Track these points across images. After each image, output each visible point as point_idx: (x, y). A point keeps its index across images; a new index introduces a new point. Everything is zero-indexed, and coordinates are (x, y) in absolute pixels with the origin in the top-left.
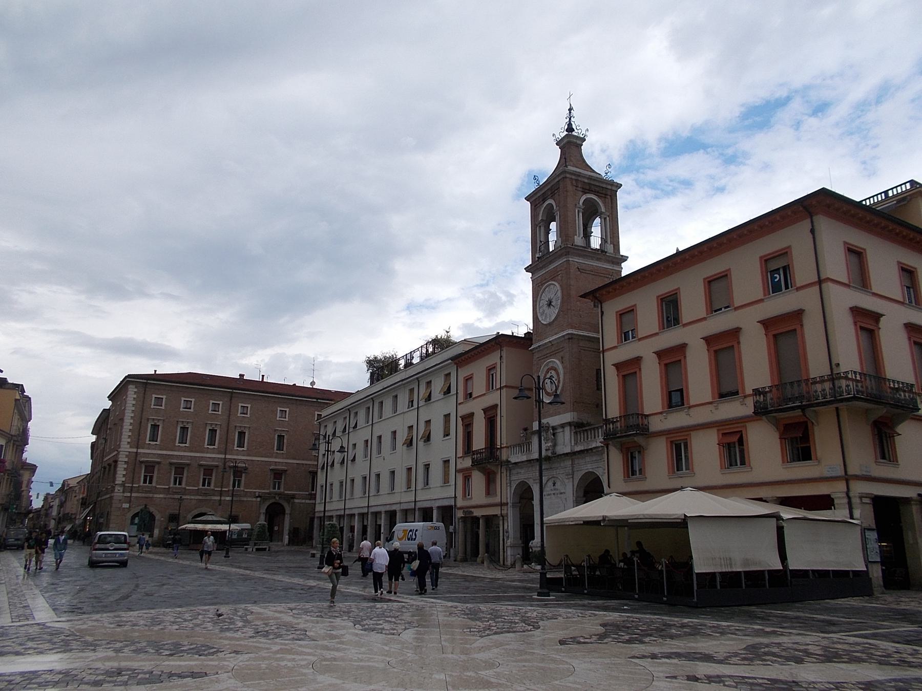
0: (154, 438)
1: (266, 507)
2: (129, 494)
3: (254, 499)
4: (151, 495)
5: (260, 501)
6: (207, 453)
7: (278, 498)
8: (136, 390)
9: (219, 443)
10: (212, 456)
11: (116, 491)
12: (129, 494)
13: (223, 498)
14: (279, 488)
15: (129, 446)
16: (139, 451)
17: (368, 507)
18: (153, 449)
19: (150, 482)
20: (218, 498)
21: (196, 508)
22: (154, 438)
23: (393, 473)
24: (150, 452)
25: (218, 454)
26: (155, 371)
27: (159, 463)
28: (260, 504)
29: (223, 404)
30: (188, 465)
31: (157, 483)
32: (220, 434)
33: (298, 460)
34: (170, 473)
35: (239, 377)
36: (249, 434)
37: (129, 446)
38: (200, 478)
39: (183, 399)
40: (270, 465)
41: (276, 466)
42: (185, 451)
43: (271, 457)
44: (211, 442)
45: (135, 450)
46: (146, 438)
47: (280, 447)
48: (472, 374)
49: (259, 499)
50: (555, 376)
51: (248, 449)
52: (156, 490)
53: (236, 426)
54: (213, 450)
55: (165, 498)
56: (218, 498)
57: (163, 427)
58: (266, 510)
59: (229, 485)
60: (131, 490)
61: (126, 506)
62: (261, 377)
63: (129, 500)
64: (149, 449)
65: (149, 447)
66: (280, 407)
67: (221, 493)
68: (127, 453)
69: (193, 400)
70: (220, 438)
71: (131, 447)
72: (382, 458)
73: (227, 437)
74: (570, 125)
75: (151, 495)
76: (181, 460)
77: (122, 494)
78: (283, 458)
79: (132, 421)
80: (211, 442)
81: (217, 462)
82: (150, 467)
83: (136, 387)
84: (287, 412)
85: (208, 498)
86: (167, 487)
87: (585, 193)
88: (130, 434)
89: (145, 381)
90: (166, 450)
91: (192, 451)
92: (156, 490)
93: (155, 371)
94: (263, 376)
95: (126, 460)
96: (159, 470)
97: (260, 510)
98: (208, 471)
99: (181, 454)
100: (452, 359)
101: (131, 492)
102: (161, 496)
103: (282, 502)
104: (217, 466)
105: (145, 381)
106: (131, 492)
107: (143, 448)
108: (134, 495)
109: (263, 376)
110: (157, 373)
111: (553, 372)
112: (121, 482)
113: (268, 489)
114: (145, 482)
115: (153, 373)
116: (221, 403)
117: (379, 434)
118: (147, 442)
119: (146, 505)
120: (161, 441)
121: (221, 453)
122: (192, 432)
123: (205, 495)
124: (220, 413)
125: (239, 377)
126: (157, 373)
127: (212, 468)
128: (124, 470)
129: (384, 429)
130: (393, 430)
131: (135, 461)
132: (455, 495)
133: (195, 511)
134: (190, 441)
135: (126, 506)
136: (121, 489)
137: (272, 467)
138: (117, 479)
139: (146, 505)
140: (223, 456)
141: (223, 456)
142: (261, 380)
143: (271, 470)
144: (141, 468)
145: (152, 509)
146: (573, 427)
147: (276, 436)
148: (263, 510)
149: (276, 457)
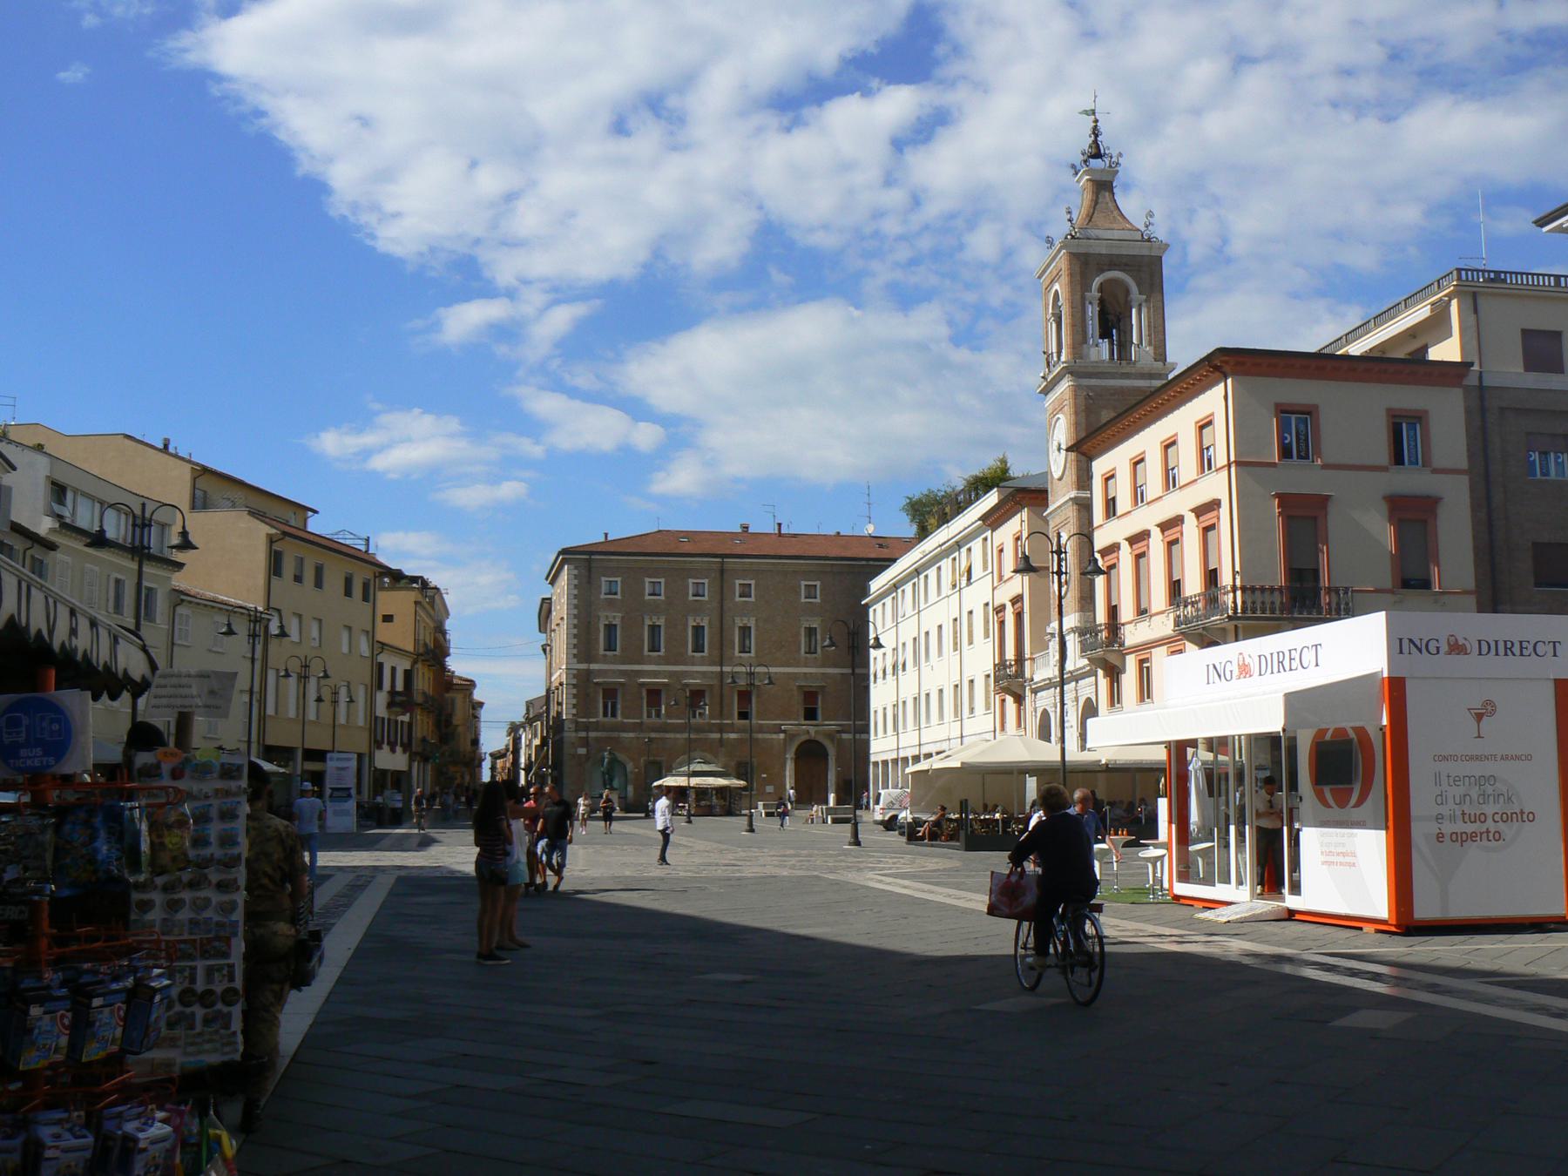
0: (610, 646)
1: (794, 750)
2: (583, 734)
3: (774, 736)
4: (615, 734)
5: (785, 739)
6: (693, 664)
7: (813, 734)
8: (576, 572)
9: (709, 648)
10: (699, 671)
11: (566, 729)
12: (583, 734)
13: (725, 736)
15: (575, 660)
17: (920, 745)
19: (614, 715)
20: (717, 736)
23: (941, 691)
25: (710, 665)
26: (606, 535)
31: (624, 716)
35: (740, 530)
36: (757, 630)
37: (575, 660)
39: (647, 580)
44: (698, 648)
45: (583, 666)
49: (782, 736)
51: (756, 652)
52: (623, 728)
54: (702, 662)
55: (638, 738)
58: (796, 754)
61: (582, 751)
62: (776, 527)
63: (585, 742)
65: (605, 660)
66: (805, 580)
67: (721, 729)
68: (575, 672)
69: (662, 580)
70: (710, 643)
72: (930, 667)
73: (722, 636)
74: (1095, 142)
75: (615, 734)
77: (574, 734)
80: (698, 648)
82: (610, 693)
83: (576, 568)
84: (818, 587)
85: (702, 736)
86: (638, 721)
87: (1103, 271)
89: (588, 557)
91: (668, 663)
92: (623, 728)
93: (606, 535)
94: (780, 525)
98: (697, 695)
99: (654, 671)
100: (984, 518)
102: (631, 735)
103: (820, 739)
105: (588, 557)
107: (596, 662)
108: (592, 734)
109: (780, 525)
110: (609, 539)
114: (605, 715)
115: (603, 540)
116: (706, 581)
117: (926, 630)
122: (666, 633)
124: (706, 598)
125: (740, 530)
126: (609, 539)
128: (574, 698)
129: (930, 620)
130: (939, 624)
132: (995, 727)
135: (582, 751)
136: (572, 726)
140: (718, 669)
141: (718, 669)
142: (777, 532)
143: (800, 687)
146: (1077, 634)
147: (803, 630)
148: (790, 755)
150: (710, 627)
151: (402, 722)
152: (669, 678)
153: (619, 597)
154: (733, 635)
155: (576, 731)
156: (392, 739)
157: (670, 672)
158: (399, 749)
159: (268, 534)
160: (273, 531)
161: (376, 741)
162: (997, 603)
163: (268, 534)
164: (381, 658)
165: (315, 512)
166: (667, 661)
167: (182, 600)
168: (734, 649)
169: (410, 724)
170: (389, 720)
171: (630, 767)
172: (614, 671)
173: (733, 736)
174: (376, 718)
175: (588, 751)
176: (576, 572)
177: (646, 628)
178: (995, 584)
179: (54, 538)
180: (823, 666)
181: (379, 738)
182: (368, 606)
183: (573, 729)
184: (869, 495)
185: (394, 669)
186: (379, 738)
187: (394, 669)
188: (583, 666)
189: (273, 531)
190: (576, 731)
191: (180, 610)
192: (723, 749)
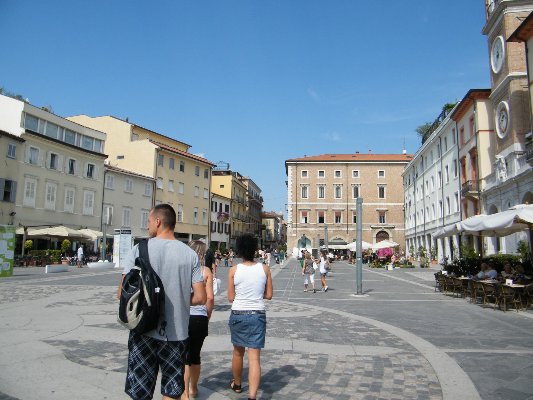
0: (305, 196)
2: (295, 229)
3: (368, 229)
4: (307, 229)
6: (336, 202)
8: (292, 168)
9: (343, 196)
12: (295, 229)
13: (349, 229)
14: (384, 222)
16: (298, 203)
18: (305, 202)
20: (346, 229)
21: (333, 236)
22: (305, 196)
24: (304, 204)
27: (310, 210)
28: (372, 232)
29: (342, 171)
30: (326, 210)
32: (343, 191)
33: (395, 202)
34: (316, 215)
37: (292, 201)
38: (333, 217)
40: (376, 207)
41: (380, 207)
42: (323, 202)
43: (377, 202)
45: (295, 203)
46: (300, 196)
47: (382, 195)
48: (463, 126)
50: (505, 116)
53: (352, 185)
56: (346, 229)
57: (309, 189)
59: (351, 221)
60: (296, 226)
61: (294, 235)
64: (303, 202)
67: (347, 227)
70: (343, 193)
71: (293, 202)
76: (322, 207)
77: (291, 229)
78: (384, 202)
79: (292, 187)
81: (343, 207)
85: (340, 229)
88: (292, 194)
90: (312, 202)
91: (327, 202)
95: (291, 209)
96: (310, 214)
97: (372, 235)
99: (322, 204)
101: (296, 227)
102: (313, 229)
103: (386, 230)
104: (343, 210)
106: (296, 227)
108: (298, 229)
111: (503, 112)
112: (290, 222)
113: (376, 223)
115: (304, 157)
118: (302, 198)
119: (304, 235)
120: (309, 197)
121: (344, 202)
122: (326, 190)
123: (338, 227)
127: (383, 211)
131: (296, 210)
133: (333, 237)
134: (326, 196)
137: (378, 209)
138: (288, 220)
139: (304, 235)
140: (346, 204)
141: (346, 204)
144: (300, 213)
145: (308, 237)
148: (374, 236)
149: (380, 202)
150: (343, 188)
151: (226, 224)
152: (327, 207)
153: (308, 177)
154: (351, 190)
155: (292, 228)
156: (221, 230)
157: (327, 205)
158: (224, 234)
159: (156, 149)
160: (157, 147)
161: (212, 231)
162: (460, 157)
163: (156, 149)
164: (214, 200)
165: (191, 147)
166: (326, 201)
167: (108, 171)
168: (352, 196)
169: (230, 225)
170: (219, 224)
171: (312, 241)
172: (306, 205)
173: (352, 229)
174: (212, 222)
175: (296, 236)
176: (292, 168)
177: (318, 189)
178: (460, 148)
179: (25, 138)
180: (387, 202)
181: (214, 229)
182: (208, 180)
183: (291, 227)
184: (404, 139)
185: (221, 205)
186: (214, 229)
187: (221, 205)
188: (295, 203)
189: (157, 147)
190: (292, 228)
191: (107, 175)
192: (348, 234)
